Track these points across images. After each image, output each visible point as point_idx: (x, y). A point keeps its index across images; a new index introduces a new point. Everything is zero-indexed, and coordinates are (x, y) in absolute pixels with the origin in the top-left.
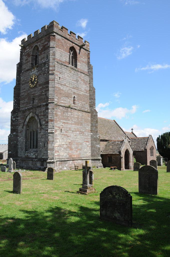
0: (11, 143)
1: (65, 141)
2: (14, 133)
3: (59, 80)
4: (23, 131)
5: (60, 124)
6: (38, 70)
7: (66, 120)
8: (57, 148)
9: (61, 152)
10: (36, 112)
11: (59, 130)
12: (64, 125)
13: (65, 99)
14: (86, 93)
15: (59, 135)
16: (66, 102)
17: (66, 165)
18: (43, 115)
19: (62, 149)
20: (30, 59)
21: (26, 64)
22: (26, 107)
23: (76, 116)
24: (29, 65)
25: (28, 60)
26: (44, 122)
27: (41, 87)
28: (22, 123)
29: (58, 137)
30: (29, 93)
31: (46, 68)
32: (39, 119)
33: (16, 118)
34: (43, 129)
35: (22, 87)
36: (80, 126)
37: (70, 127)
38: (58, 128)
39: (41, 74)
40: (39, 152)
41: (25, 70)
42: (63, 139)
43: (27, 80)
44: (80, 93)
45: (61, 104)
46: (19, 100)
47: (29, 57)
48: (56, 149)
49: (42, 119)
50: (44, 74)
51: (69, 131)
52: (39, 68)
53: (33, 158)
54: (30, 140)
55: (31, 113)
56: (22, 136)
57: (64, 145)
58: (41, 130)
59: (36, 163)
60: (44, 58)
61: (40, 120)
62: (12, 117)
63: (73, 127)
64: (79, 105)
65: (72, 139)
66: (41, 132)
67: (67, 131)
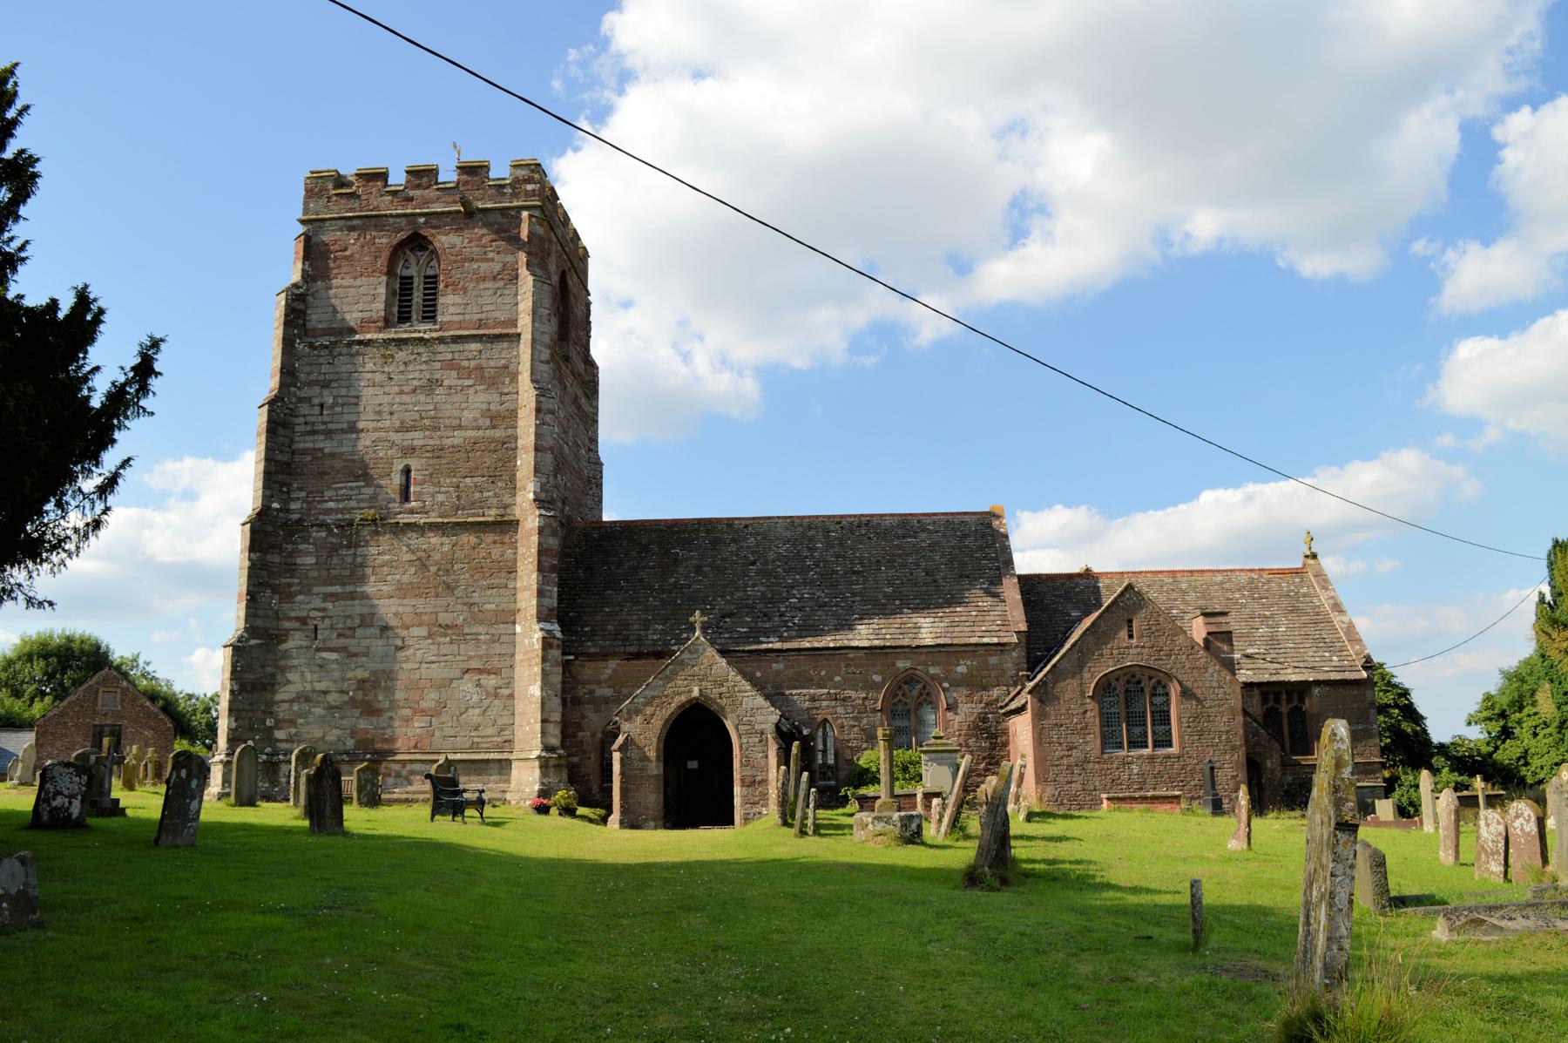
1: (336, 675)
5: (309, 606)
7: (343, 584)
8: (286, 706)
9: (308, 724)
11: (298, 633)
12: (330, 606)
13: (349, 492)
14: (494, 427)
15: (302, 651)
16: (353, 504)
29: (295, 662)
44: (448, 442)
45: (321, 517)
48: (283, 711)
51: (359, 632)
57: (325, 693)
64: (441, 498)
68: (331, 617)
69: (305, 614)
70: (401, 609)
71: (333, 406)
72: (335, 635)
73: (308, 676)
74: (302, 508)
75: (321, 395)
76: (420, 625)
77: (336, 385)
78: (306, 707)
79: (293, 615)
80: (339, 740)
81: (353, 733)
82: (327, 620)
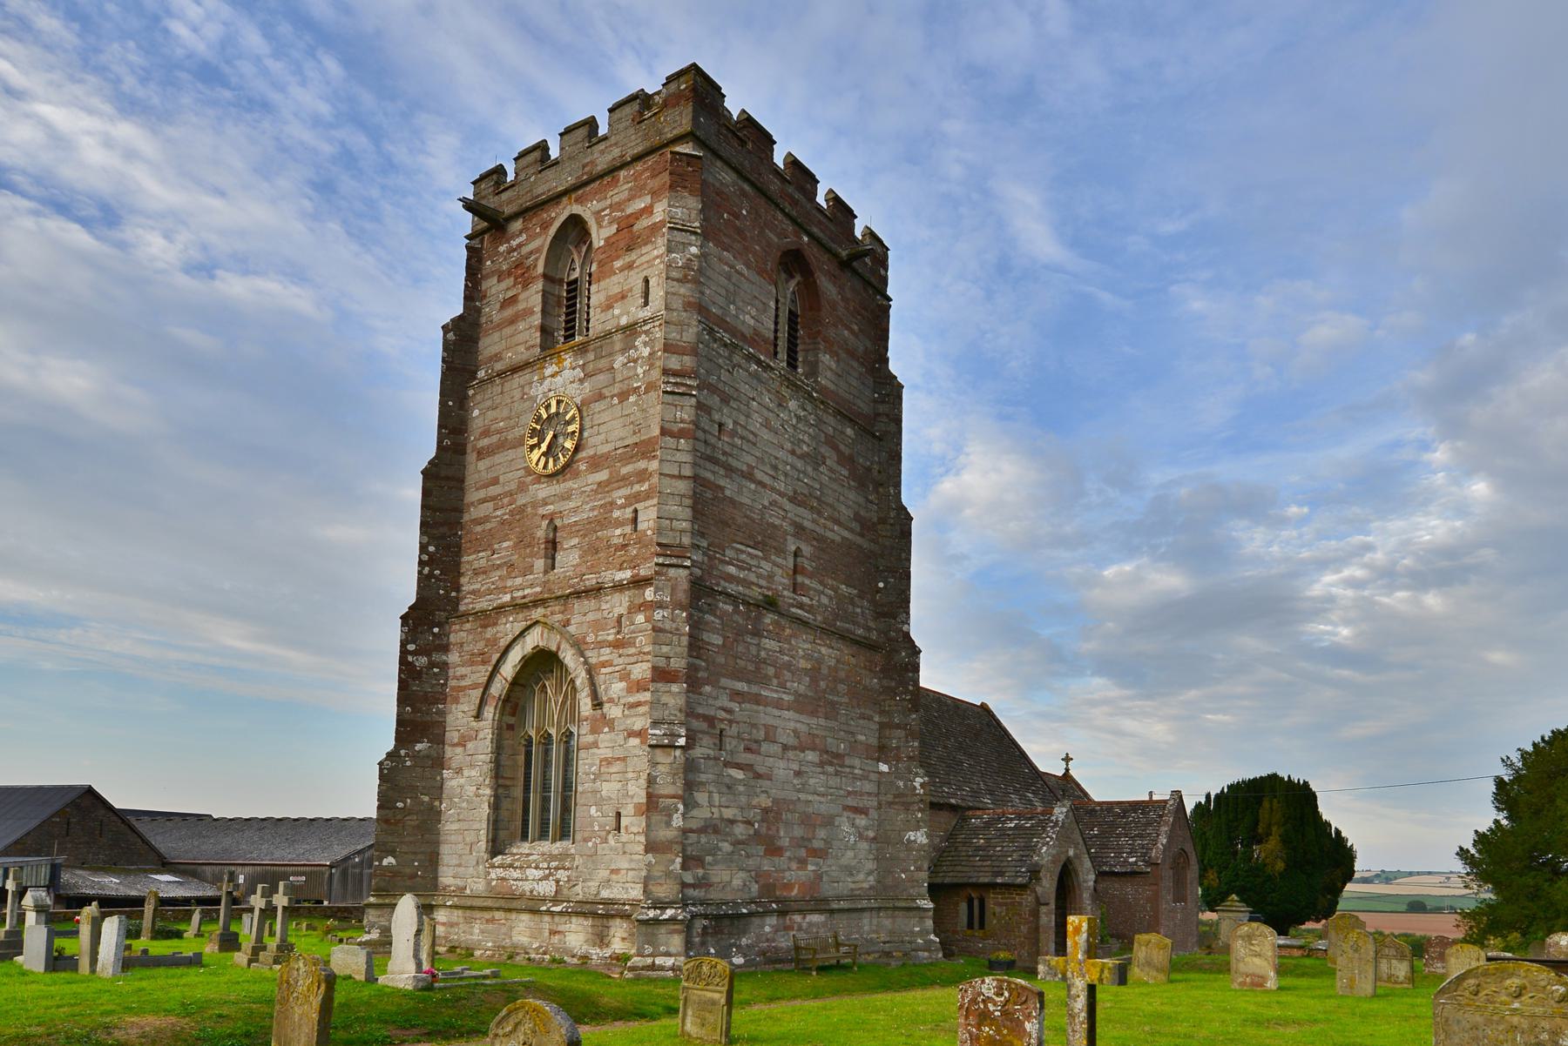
0: (400, 805)
1: (743, 799)
2: (419, 747)
3: (713, 440)
4: (481, 735)
5: (719, 703)
6: (583, 367)
7: (749, 682)
9: (716, 862)
10: (567, 623)
12: (735, 706)
17: (744, 941)
18: (617, 645)
19: (726, 847)
20: (533, 298)
21: (508, 331)
22: (504, 590)
23: (803, 664)
24: (527, 335)
25: (521, 306)
26: (623, 684)
27: (603, 475)
28: (474, 686)
30: (522, 509)
31: (635, 361)
32: (586, 663)
33: (435, 657)
34: (610, 723)
35: (477, 469)
36: (822, 721)
37: (770, 721)
38: (704, 726)
39: (606, 392)
40: (578, 861)
41: (499, 366)
42: (729, 787)
43: (507, 429)
45: (722, 582)
46: (459, 546)
47: (526, 286)
49: (604, 665)
50: (623, 396)
51: (765, 747)
52: (591, 356)
53: (544, 900)
54: (518, 792)
55: (538, 630)
56: (472, 766)
57: (732, 822)
58: (595, 730)
59: (561, 928)
60: (623, 297)
61: (591, 671)
62: (411, 647)
63: (789, 723)
65: (781, 795)
66: (595, 745)
67: (754, 746)
68: (738, 723)
69: (712, 713)
70: (798, 725)
71: (733, 434)
72: (742, 747)
73: (716, 797)
74: (703, 563)
75: (720, 410)
76: (813, 749)
77: (734, 406)
78: (714, 839)
79: (700, 710)
80: (745, 885)
81: (758, 876)
82: (734, 725)
